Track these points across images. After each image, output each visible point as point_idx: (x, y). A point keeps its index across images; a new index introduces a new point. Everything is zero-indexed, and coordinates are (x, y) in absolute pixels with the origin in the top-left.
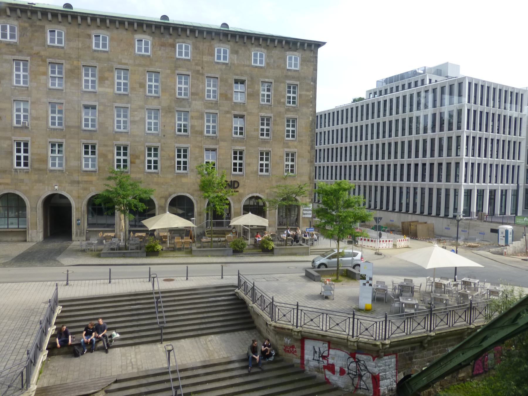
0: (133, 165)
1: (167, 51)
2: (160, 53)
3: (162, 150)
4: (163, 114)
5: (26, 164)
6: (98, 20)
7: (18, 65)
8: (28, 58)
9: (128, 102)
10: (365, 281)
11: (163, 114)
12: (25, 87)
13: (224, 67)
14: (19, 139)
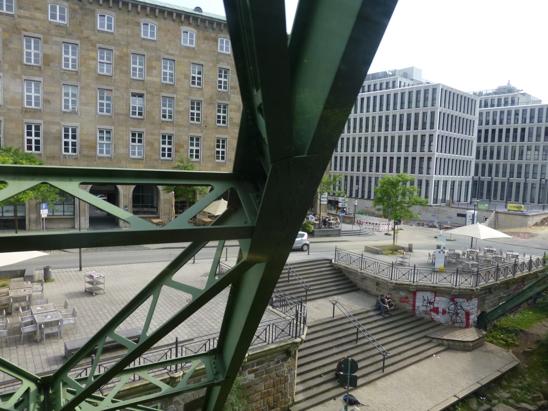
0: (177, 153)
1: (210, 45)
2: (203, 46)
3: (204, 140)
4: (205, 106)
5: (74, 151)
6: (148, 9)
7: (28, 42)
8: (78, 42)
9: (175, 92)
10: (440, 250)
11: (205, 106)
12: (75, 71)
14: (68, 124)
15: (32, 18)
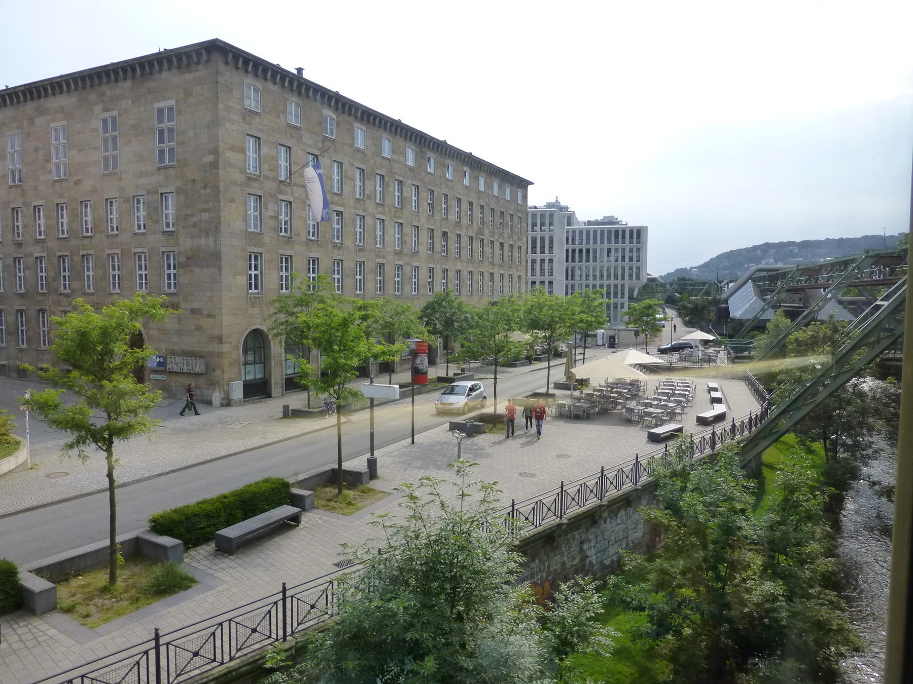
9: (461, 230)
15: (398, 162)
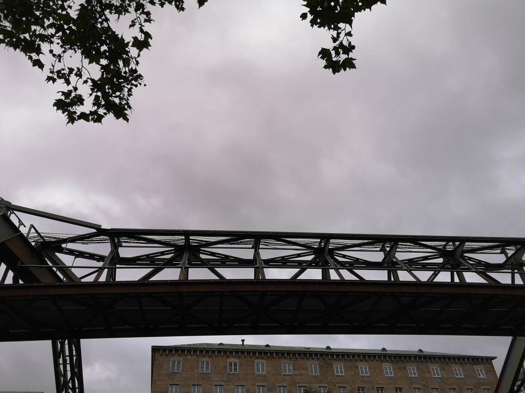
13: (439, 380)
